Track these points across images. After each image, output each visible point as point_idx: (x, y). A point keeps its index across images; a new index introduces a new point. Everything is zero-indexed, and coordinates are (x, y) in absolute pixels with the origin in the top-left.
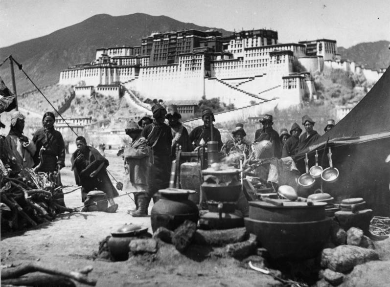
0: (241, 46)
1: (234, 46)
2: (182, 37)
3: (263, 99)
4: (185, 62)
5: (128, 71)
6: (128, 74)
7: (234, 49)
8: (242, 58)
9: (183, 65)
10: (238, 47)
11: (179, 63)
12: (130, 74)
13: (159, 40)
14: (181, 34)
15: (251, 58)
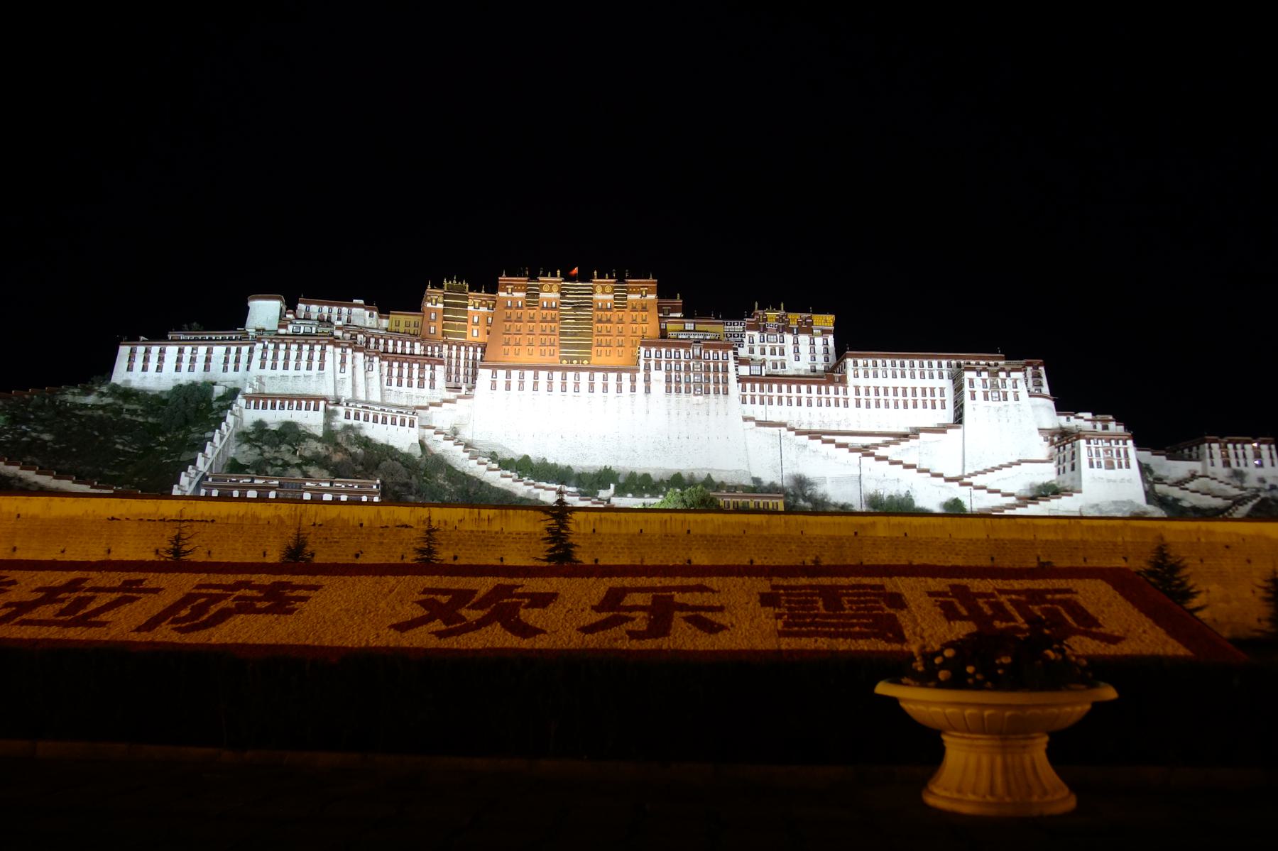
0: (782, 353)
1: (757, 350)
2: (611, 297)
3: (1012, 495)
4: (663, 364)
5: (422, 369)
6: (421, 379)
7: (757, 355)
8: (843, 381)
9: (658, 377)
10: (773, 352)
11: (642, 363)
12: (427, 383)
13: (523, 294)
14: (608, 289)
15: (872, 382)
